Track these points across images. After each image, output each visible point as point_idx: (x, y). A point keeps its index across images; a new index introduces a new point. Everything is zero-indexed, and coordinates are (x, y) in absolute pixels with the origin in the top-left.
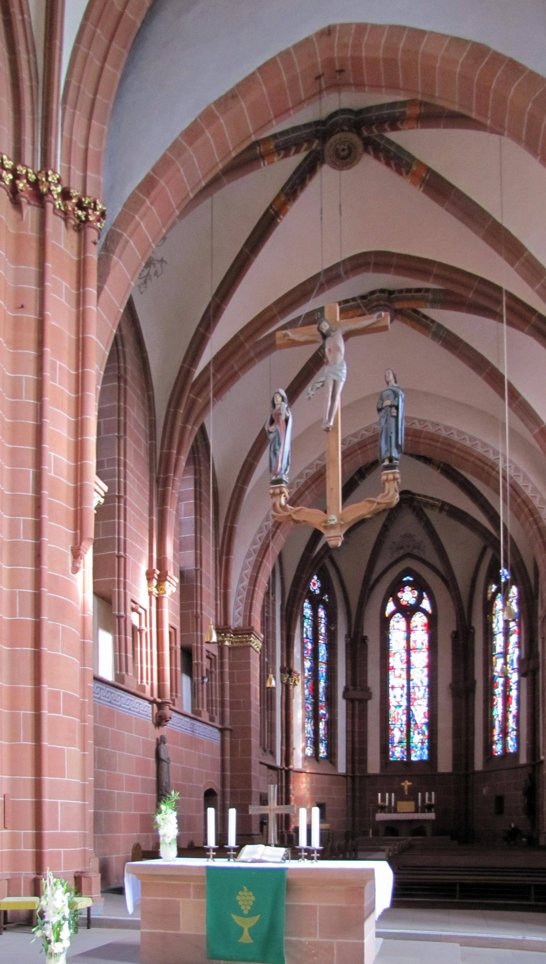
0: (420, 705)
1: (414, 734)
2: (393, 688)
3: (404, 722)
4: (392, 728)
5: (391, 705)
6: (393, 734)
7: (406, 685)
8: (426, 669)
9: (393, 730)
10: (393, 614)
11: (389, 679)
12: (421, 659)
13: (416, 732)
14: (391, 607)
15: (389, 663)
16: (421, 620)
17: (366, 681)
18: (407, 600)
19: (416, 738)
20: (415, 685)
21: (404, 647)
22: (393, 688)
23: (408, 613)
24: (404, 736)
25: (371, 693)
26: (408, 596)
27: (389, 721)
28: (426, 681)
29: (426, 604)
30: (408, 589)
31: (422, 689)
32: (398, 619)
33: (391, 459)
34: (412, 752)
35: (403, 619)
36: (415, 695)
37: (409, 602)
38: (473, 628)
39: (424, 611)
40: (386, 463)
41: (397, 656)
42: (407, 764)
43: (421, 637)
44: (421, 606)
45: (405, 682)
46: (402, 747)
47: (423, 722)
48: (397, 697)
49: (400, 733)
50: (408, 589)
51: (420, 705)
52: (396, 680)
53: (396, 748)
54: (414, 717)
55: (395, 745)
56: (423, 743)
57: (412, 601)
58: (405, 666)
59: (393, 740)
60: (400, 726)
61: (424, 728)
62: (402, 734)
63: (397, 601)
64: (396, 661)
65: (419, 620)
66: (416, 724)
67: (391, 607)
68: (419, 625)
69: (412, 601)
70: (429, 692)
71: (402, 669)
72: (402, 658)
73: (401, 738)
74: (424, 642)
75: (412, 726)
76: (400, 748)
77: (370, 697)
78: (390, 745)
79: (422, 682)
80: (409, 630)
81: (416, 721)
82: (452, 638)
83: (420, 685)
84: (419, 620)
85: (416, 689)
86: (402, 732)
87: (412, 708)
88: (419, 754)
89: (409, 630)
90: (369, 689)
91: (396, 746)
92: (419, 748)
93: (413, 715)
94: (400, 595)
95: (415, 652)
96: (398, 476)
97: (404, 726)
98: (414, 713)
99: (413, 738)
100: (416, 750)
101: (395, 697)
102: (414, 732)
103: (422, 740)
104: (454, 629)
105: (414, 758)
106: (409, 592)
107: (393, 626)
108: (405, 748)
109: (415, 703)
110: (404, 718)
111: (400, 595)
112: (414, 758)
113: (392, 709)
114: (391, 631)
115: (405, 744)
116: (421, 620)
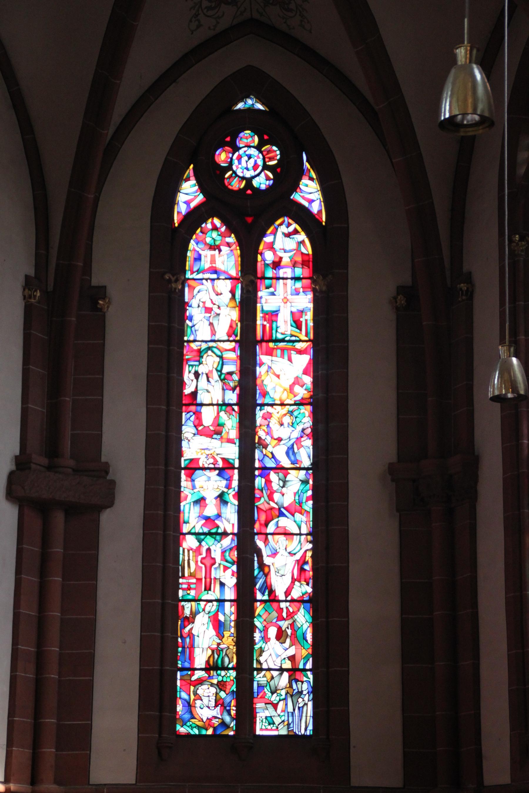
0: (288, 534)
1: (266, 639)
2: (193, 468)
3: (230, 594)
4: (187, 612)
5: (185, 529)
6: (191, 635)
7: (237, 465)
8: (306, 411)
9: (190, 620)
10: (195, 218)
11: (179, 440)
12: (286, 375)
13: (272, 632)
14: (189, 194)
15: (182, 384)
16: (291, 244)
17: (97, 440)
18: (248, 174)
19: (273, 653)
20: (270, 464)
21: (231, 332)
22: (193, 468)
23: (249, 220)
24: (229, 641)
25: (112, 486)
26: (248, 163)
27: (176, 587)
28: (305, 455)
29: (310, 193)
30: (248, 138)
31: (295, 478)
32: (215, 234)
34: (259, 706)
35: (231, 239)
36: (271, 498)
37: (255, 183)
38: (469, 279)
39: (303, 216)
41: (210, 362)
42: (239, 744)
43: (288, 302)
44: (297, 197)
45: (232, 452)
46: (221, 686)
47: (296, 594)
48: (205, 498)
49: (212, 632)
50: (248, 138)
51: (288, 534)
52: (205, 446)
53: (203, 690)
54: (267, 575)
55: (198, 674)
56: (294, 672)
58: (232, 397)
59: (192, 658)
60: (213, 607)
61: (303, 619)
62: (220, 636)
63: (212, 179)
64: (208, 383)
65: (285, 242)
66: (273, 599)
67: (189, 194)
68: (286, 260)
70: (314, 489)
71: (225, 405)
72: (226, 369)
73: (217, 650)
74: (303, 320)
75: (259, 608)
76: (213, 690)
77: (109, 502)
78: (179, 673)
79: (290, 452)
80: (250, 280)
81: (272, 592)
82: (397, 309)
83: (286, 463)
84: (285, 242)
85: (273, 476)
86: (218, 626)
87: (260, 544)
88: (284, 713)
89: (250, 280)
90: (105, 469)
91: (200, 682)
92: (283, 693)
93: (262, 566)
94: (222, 157)
95: (270, 352)
97: (229, 609)
98: (267, 561)
99: (261, 651)
100: (274, 698)
101: (201, 501)
102: (266, 629)
103: (292, 658)
104: (406, 279)
105: (261, 729)
106: (253, 152)
107: (198, 258)
108: (234, 688)
109: (271, 528)
110: (230, 580)
111: (222, 157)
112: (261, 729)
113: (190, 542)
114: (188, 275)
115: (233, 674)
116: (291, 244)
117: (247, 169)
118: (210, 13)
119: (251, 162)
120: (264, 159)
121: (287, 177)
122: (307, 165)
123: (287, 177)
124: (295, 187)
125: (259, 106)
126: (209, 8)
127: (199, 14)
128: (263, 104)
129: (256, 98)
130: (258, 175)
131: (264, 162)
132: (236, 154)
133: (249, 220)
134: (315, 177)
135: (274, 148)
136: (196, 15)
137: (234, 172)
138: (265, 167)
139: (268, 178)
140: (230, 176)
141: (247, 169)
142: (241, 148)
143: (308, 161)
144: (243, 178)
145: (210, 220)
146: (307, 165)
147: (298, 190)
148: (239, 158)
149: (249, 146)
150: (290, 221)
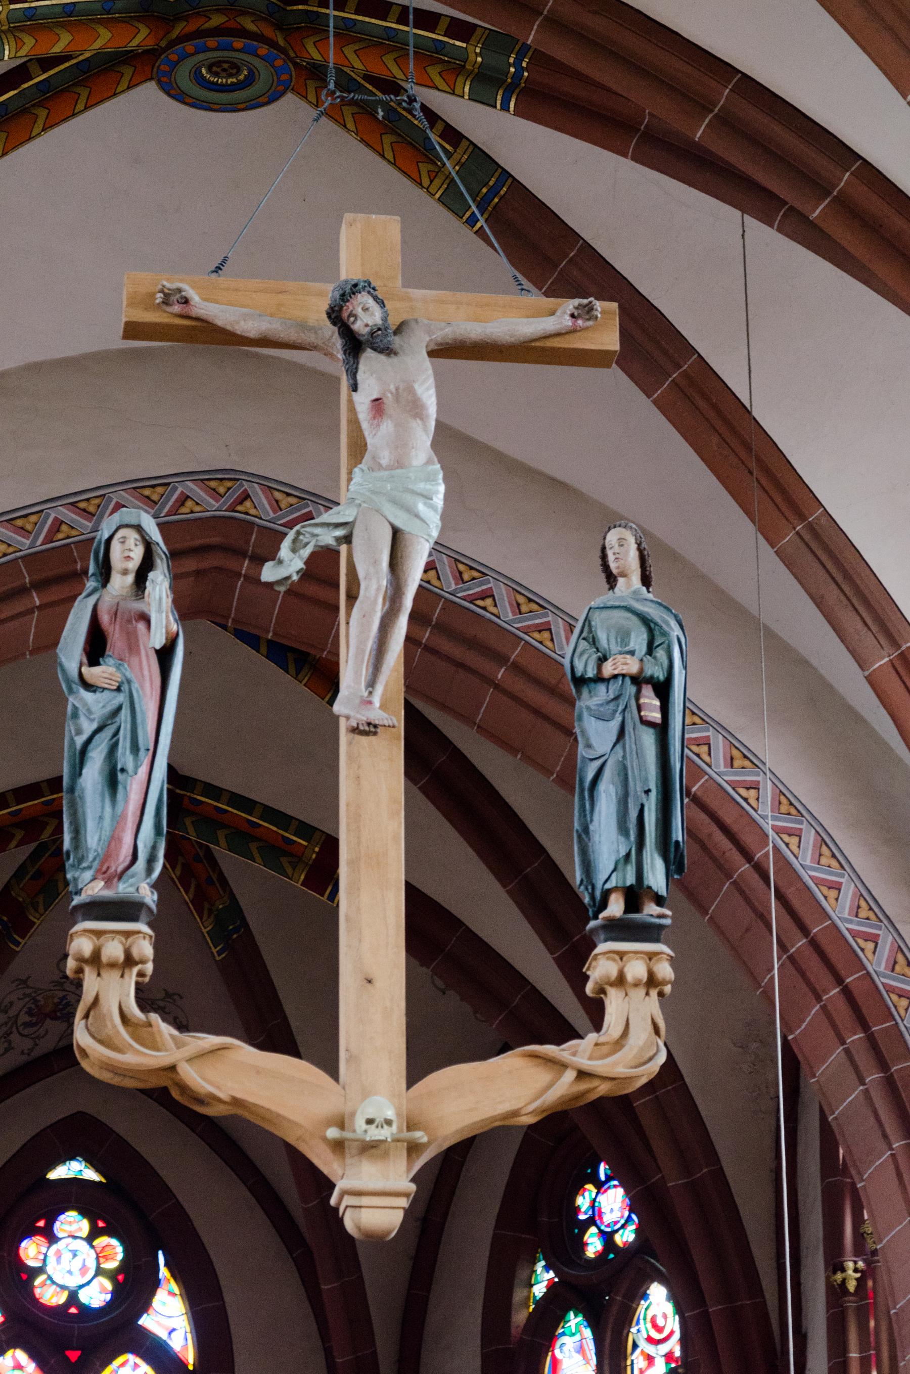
18: (72, 1282)
23: (73, 1355)
30: (72, 1223)
33: (635, 896)
37: (84, 1297)
40: (616, 908)
44: (146, 1321)
50: (72, 1223)
57: (96, 1295)
69: (96, 1295)
94: (31, 1250)
96: (665, 970)
106: (83, 1246)
117: (70, 1272)
118: (26, 1032)
119: (77, 1264)
120: (98, 1258)
121: (134, 1288)
122: (164, 1272)
123: (134, 1288)
124: (145, 1306)
125: (91, 1175)
126: (27, 1025)
127: (11, 1033)
128: (97, 1170)
129: (86, 1160)
130: (88, 1283)
131: (98, 1264)
132: (54, 1247)
133: (73, 1355)
134: (177, 1291)
135: (114, 1242)
136: (8, 1034)
137: (50, 1278)
138: (99, 1272)
139: (103, 1290)
140: (43, 1284)
141: (70, 1272)
142: (59, 1239)
143: (166, 1265)
144: (63, 1288)
145: (10, 1353)
146: (164, 1272)
147: (151, 1311)
148: (59, 1254)
149: (75, 1237)
150: (139, 1361)
